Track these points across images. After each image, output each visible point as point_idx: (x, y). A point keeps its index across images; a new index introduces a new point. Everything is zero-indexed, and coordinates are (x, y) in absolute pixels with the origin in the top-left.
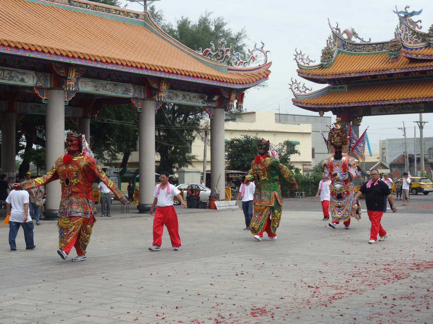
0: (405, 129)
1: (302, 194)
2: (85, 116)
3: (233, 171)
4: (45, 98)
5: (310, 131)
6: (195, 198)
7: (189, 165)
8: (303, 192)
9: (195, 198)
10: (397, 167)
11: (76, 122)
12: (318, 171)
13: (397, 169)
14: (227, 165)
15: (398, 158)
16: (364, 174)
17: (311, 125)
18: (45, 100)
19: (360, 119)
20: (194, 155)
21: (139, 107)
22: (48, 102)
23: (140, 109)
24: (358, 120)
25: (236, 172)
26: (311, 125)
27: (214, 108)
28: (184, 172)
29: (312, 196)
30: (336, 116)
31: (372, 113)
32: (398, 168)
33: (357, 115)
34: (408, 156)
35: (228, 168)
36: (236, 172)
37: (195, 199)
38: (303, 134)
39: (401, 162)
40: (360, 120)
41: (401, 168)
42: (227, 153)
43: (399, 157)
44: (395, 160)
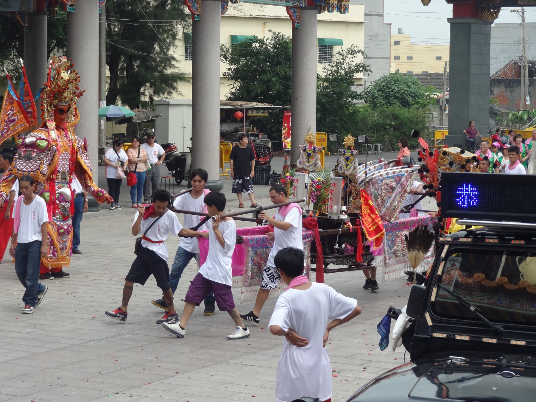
0: (523, 13)
1: (376, 147)
2: (39, 11)
3: (254, 104)
4: (70, 3)
5: (361, 18)
6: (264, 167)
7: (174, 92)
8: (379, 145)
9: (264, 167)
10: (502, 85)
11: (24, 21)
12: (376, 98)
13: (503, 89)
14: (233, 90)
15: (505, 67)
16: (496, 114)
17: (363, 7)
18: (71, 6)
19: (496, 13)
20: (182, 72)
21: (196, 13)
22: (74, 9)
23: (198, 15)
24: (492, 15)
25: (260, 105)
26: (363, 7)
27: (301, 8)
28: (168, 105)
29: (389, 150)
30: (451, 6)
31: (519, 2)
32: (506, 87)
33: (491, 5)
34: (527, 65)
35: (236, 97)
36: (260, 105)
37: (263, 169)
38: (348, 24)
39: (510, 75)
40: (495, 15)
41: (511, 87)
42: (234, 67)
43: (507, 65)
44: (500, 70)
